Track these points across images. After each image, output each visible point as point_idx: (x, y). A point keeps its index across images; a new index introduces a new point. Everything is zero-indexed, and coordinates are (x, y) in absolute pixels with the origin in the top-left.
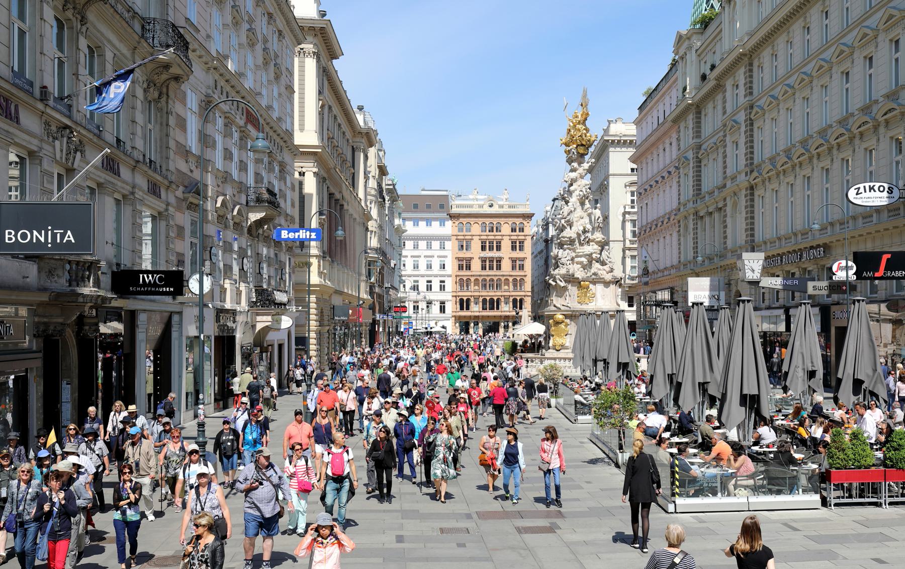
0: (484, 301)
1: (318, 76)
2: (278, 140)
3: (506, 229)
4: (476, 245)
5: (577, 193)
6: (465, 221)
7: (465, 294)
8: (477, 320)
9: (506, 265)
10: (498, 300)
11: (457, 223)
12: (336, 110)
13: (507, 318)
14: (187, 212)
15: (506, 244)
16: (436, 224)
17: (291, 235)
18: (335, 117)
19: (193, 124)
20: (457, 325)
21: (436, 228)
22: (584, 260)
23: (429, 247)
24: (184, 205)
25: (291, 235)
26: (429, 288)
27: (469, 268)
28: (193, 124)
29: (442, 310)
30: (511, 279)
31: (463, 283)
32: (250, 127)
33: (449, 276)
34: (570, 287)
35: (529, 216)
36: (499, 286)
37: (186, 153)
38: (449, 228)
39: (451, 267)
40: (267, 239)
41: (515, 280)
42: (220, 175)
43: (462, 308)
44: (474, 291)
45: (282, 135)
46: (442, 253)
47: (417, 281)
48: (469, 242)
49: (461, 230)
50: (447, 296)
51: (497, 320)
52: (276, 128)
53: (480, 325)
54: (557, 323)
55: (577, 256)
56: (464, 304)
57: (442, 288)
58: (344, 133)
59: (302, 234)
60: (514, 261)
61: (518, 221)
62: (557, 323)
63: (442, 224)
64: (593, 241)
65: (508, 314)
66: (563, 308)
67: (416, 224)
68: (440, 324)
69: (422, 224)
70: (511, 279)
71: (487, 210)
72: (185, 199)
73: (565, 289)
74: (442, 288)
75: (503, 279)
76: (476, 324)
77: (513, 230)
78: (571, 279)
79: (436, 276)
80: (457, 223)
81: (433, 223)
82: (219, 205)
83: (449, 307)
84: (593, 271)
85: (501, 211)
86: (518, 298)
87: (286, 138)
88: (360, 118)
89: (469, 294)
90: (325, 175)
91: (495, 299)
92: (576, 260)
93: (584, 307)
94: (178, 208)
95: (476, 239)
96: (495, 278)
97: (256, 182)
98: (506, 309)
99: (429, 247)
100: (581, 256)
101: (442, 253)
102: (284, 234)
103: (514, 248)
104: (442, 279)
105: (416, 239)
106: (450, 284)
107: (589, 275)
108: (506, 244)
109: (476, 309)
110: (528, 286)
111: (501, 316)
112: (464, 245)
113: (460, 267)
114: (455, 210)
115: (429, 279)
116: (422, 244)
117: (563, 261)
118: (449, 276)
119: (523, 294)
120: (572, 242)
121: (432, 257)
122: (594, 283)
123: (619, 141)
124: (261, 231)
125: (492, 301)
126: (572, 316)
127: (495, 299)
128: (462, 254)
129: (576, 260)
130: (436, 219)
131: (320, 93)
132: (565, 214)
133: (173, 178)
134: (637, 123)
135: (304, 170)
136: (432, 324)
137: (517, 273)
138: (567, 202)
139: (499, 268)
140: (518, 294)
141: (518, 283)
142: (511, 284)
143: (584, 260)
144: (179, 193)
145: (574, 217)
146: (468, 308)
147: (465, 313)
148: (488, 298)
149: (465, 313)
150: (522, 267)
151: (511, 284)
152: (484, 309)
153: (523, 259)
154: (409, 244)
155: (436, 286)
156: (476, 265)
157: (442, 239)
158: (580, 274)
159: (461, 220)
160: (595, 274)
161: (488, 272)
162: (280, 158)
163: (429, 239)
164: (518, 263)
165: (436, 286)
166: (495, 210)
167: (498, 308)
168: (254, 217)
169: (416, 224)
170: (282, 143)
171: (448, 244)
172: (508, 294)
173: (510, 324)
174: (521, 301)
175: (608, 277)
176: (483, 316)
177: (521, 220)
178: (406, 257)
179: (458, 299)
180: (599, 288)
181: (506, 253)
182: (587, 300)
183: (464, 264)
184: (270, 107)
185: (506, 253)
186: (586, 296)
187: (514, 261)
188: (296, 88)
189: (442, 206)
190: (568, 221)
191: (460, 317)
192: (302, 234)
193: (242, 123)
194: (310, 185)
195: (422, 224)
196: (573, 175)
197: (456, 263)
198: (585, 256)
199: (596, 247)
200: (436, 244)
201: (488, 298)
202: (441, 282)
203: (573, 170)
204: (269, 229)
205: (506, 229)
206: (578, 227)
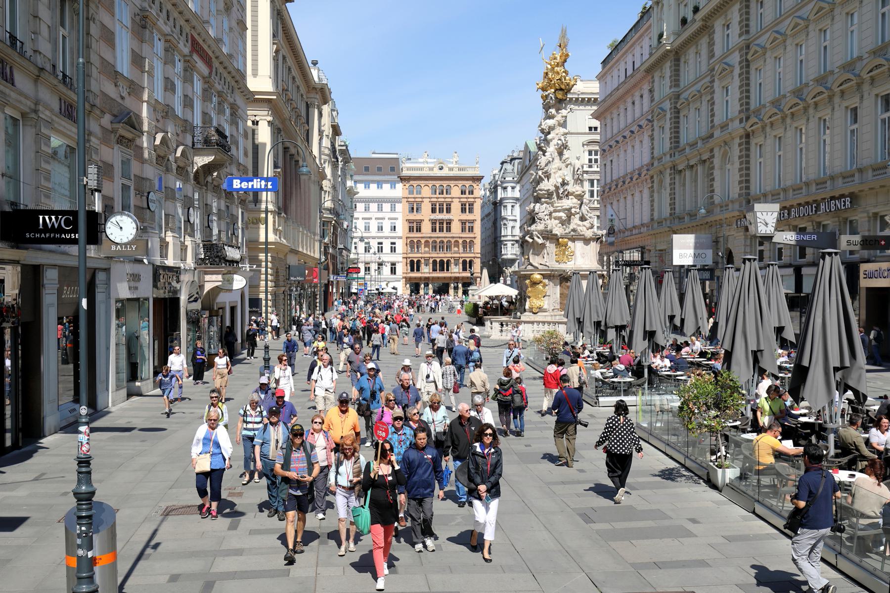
0: (435, 262)
1: (272, 17)
2: (229, 79)
3: (456, 192)
4: (426, 207)
5: (555, 142)
6: (415, 183)
7: (415, 256)
8: (427, 281)
9: (456, 227)
10: (448, 262)
11: (408, 185)
12: (290, 62)
13: (457, 280)
14: (116, 147)
15: (456, 207)
16: (387, 186)
17: (244, 185)
18: (290, 69)
19: (124, 43)
20: (408, 286)
21: (386, 191)
22: (563, 215)
23: (380, 209)
24: (113, 139)
25: (244, 185)
26: (380, 250)
27: (419, 230)
28: (124, 43)
29: (393, 271)
30: (461, 241)
31: (413, 245)
32: (195, 57)
33: (400, 238)
34: (548, 244)
35: (478, 179)
36: (449, 248)
37: (115, 75)
38: (400, 190)
39: (402, 229)
40: (217, 189)
41: (464, 242)
42: (160, 107)
43: (412, 270)
44: (424, 253)
45: (234, 73)
46: (393, 215)
47: (369, 243)
48: (419, 205)
49: (411, 192)
50: (397, 258)
51: (446, 282)
52: (227, 64)
53: (430, 286)
54: (535, 284)
55: (555, 211)
56: (414, 265)
57: (393, 250)
58: (298, 87)
59: (256, 184)
60: (463, 223)
61: (468, 183)
62: (535, 284)
63: (393, 186)
64: (572, 194)
65: (458, 275)
66: (540, 267)
67: (367, 186)
68: (391, 285)
69: (373, 186)
70: (461, 241)
71: (437, 173)
72: (114, 131)
73: (543, 246)
74: (393, 250)
75: (453, 240)
76: (427, 285)
77: (463, 192)
78: (549, 236)
79: (387, 238)
80: (408, 185)
81: (384, 185)
82: (158, 142)
83: (400, 269)
84: (572, 226)
85: (451, 174)
86: (468, 260)
87: (238, 78)
88: (315, 73)
89: (420, 255)
90: (280, 126)
91: (445, 260)
92: (554, 215)
93: (562, 266)
94: (105, 141)
95: (426, 201)
96: (445, 240)
97: (204, 122)
98: (456, 271)
99: (380, 209)
100: (559, 211)
101: (393, 215)
102: (236, 184)
103: (463, 210)
104: (393, 241)
105: (367, 201)
106: (400, 246)
107: (567, 231)
108: (456, 207)
109: (426, 271)
110: (477, 248)
111: (450, 278)
112: (414, 207)
113: (411, 229)
114: (405, 173)
115: (380, 241)
116: (374, 206)
117: (541, 215)
118: (400, 238)
119: (472, 255)
120: (549, 195)
121: (384, 219)
122: (573, 240)
123: (577, 99)
124: (209, 179)
125: (442, 262)
126: (550, 276)
127: (445, 260)
128: (413, 216)
129: (554, 215)
130: (387, 182)
131: (274, 36)
132: (543, 164)
133: (98, 102)
134: (601, 78)
135: (257, 118)
136: (384, 285)
137: (467, 235)
138: (544, 152)
139: (449, 230)
140: (468, 256)
141: (468, 245)
142: (461, 246)
143: (563, 215)
144: (106, 120)
145: (552, 168)
146: (418, 270)
147: (415, 275)
148: (438, 260)
149: (415, 275)
150: (471, 229)
151: (461, 246)
152: (434, 270)
153: (473, 221)
154: (360, 206)
155: (387, 247)
156: (426, 227)
157: (393, 201)
158: (558, 230)
159: (412, 182)
160: (574, 230)
161: (438, 234)
162: (231, 100)
163: (380, 201)
164: (468, 225)
165: (387, 247)
166: (445, 172)
167: (448, 270)
168: (201, 161)
169: (367, 186)
170: (233, 83)
171: (399, 207)
173: (460, 285)
174: (471, 262)
175: (589, 234)
176: (433, 278)
177: (470, 183)
178: (358, 219)
179: (409, 260)
180: (579, 245)
181: (456, 215)
182: (565, 259)
183: (415, 226)
184: (218, 41)
185: (456, 215)
186: (564, 254)
187: (463, 223)
188: (249, 24)
189: (393, 169)
190: (546, 172)
191: (410, 278)
192: (256, 184)
193: (186, 50)
194: (264, 135)
195: (373, 186)
196: (550, 122)
197: (407, 225)
198: (563, 210)
199: (575, 200)
200: (387, 207)
201: (438, 260)
202: (392, 243)
203: (552, 117)
204: (219, 176)
205: (456, 192)
206: (556, 179)
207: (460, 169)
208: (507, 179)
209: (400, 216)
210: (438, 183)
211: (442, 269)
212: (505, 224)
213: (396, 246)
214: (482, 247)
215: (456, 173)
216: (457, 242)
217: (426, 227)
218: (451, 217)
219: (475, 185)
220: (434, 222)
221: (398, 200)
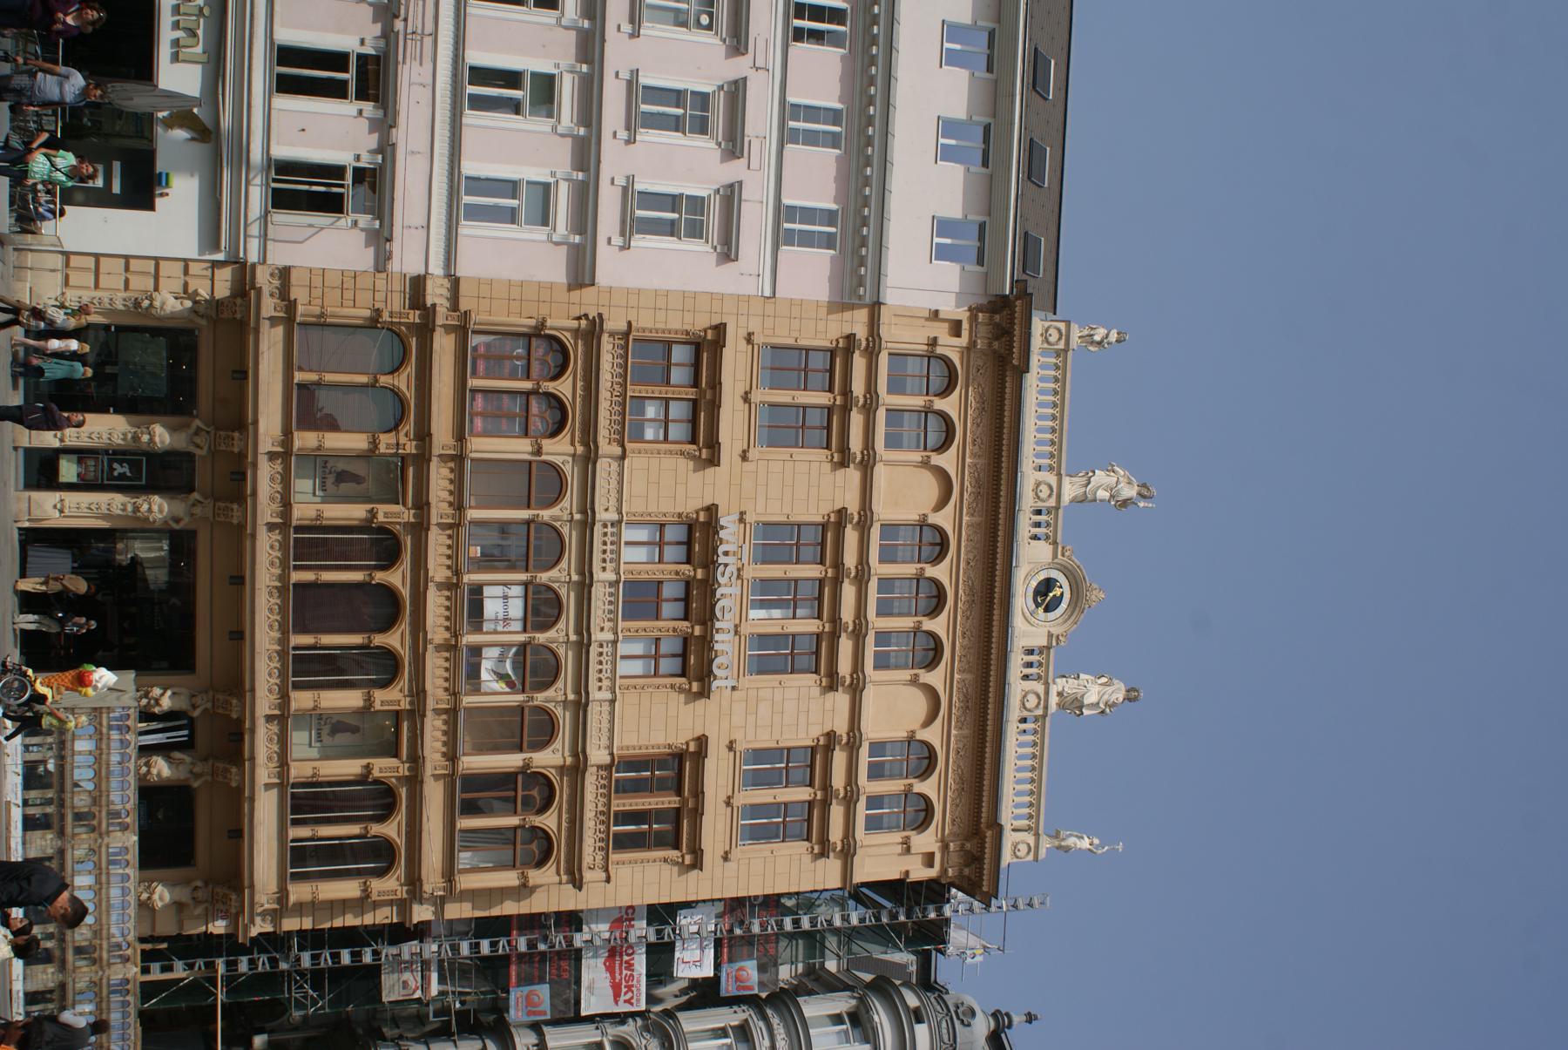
11: (951, 347)
15: (795, 711)
21: (927, 185)
29: (308, 190)
30: (548, 759)
38: (925, 286)
39: (654, 278)
46: (755, 221)
57: (501, 200)
70: (548, 759)
74: (501, 200)
79: (586, 154)
91: (394, 639)
95: (843, 489)
103: (767, 765)
111: (236, 683)
118: (582, 271)
121: (734, 146)
127: (394, 639)
176: (239, 538)
205: (894, 708)
208: (922, 1031)
209: (744, 277)
211: (307, 606)
218: (722, 680)
219: (926, 841)
220: (699, 536)
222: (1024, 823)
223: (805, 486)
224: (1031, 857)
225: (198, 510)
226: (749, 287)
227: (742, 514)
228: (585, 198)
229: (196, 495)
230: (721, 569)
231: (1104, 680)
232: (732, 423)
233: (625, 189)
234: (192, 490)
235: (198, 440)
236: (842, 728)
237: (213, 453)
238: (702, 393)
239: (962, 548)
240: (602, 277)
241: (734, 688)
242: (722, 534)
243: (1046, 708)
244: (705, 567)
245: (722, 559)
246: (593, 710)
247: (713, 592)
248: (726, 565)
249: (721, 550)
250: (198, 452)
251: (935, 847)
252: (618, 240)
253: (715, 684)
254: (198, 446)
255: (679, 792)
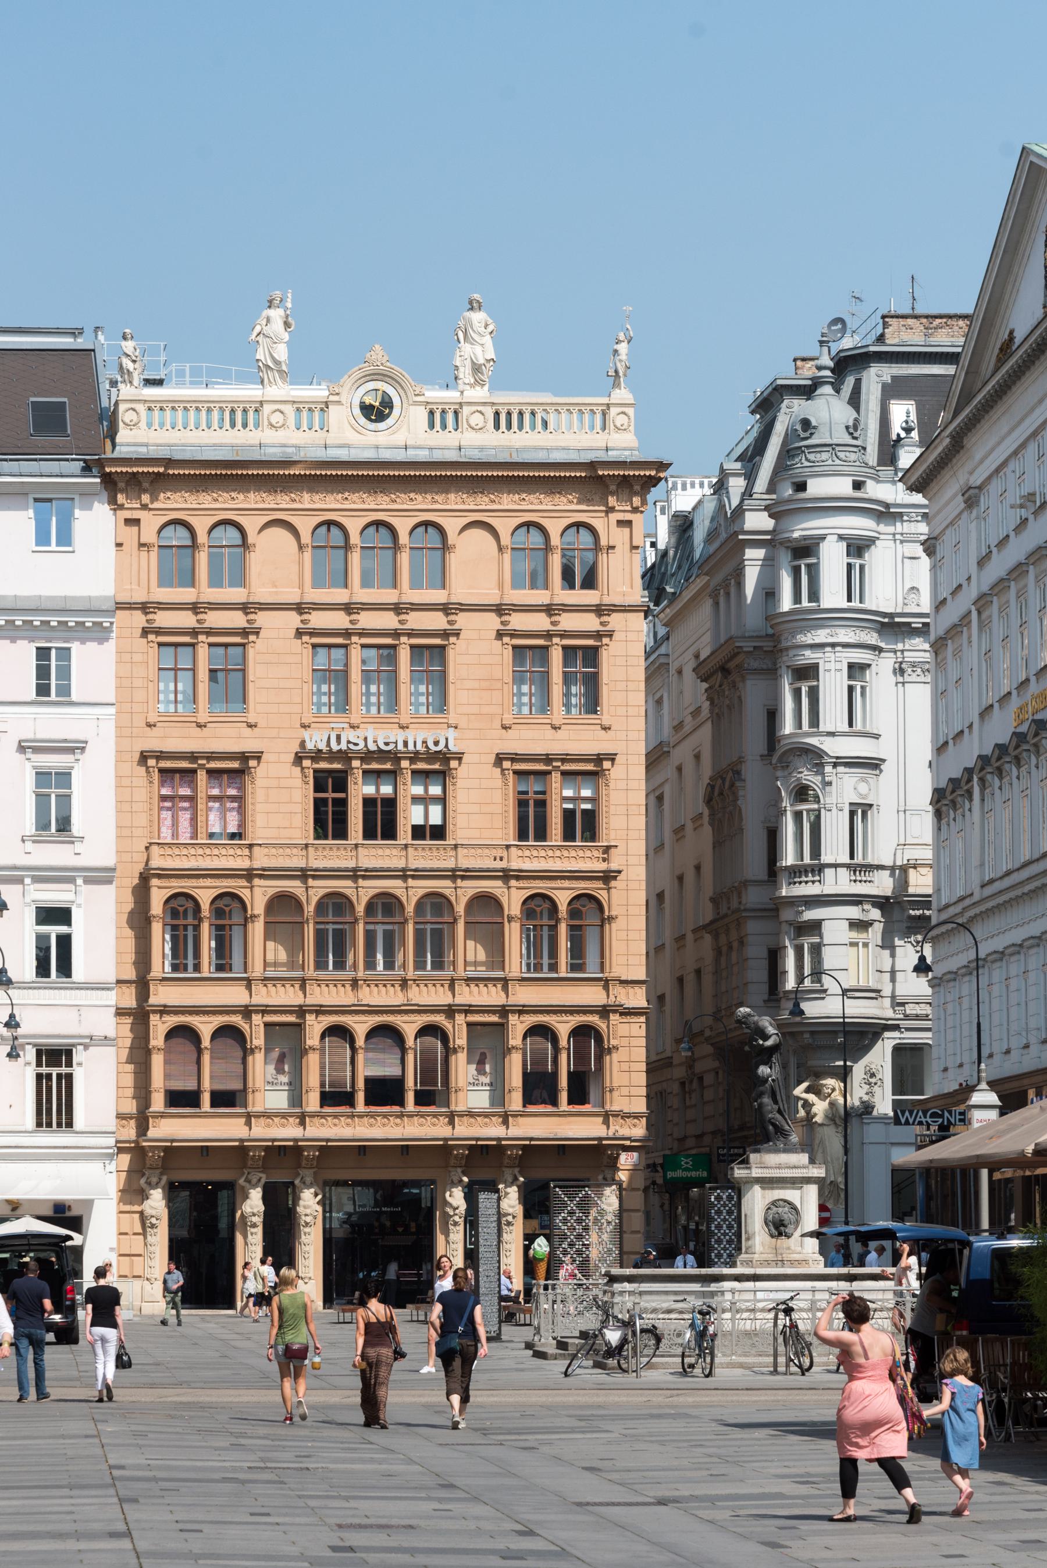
3: (478, 567)
13: (484, 1165)
20: (156, 1202)
33: (99, 876)
61: (557, 512)
71: (349, 438)
83: (100, 1088)
96: (411, 894)
98: (478, 1106)
104: (54, 895)
106: (99, 940)
108: (478, 656)
110: (629, 945)
114: (138, 436)
119: (592, 995)
153: (594, 769)
172: (493, 996)
185: (483, 714)
189: (49, 419)
191: (174, 1154)
205: (478, 567)
207: (503, 419)
210: (355, 510)
212: (802, 793)
213: (78, 930)
214: (655, 952)
215: (477, 440)
216: (486, 902)
217: (281, 806)
221: (86, 622)
222: (598, 417)
223: (279, 664)
224: (631, 411)
225: (308, 1180)
226: (109, 728)
227: (304, 726)
228: (46, 876)
229: (297, 1182)
230: (351, 746)
231: (461, 335)
232: (226, 738)
233: (34, 842)
234: (292, 1183)
235: (254, 1181)
236: (493, 621)
237: (264, 1168)
238: (202, 766)
239: (330, 503)
240: (110, 862)
241: (456, 728)
242: (322, 746)
243: (484, 404)
244: (350, 759)
245: (343, 746)
246: (464, 864)
247: (369, 752)
248: (349, 742)
249: (335, 747)
250: (263, 1181)
251: (614, 517)
252: (78, 847)
253: (452, 747)
254: (259, 1180)
255: (549, 773)
